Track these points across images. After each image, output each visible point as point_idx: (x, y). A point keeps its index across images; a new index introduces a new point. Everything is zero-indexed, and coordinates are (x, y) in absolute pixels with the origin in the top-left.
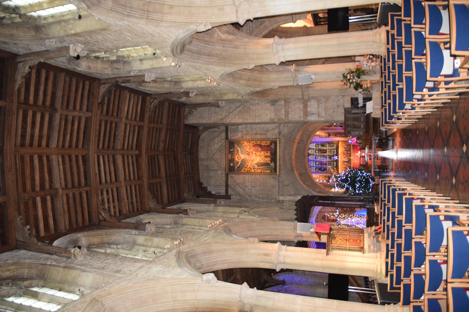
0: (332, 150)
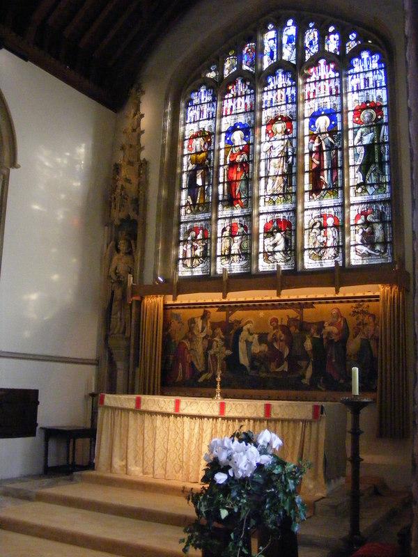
0: (330, 232)
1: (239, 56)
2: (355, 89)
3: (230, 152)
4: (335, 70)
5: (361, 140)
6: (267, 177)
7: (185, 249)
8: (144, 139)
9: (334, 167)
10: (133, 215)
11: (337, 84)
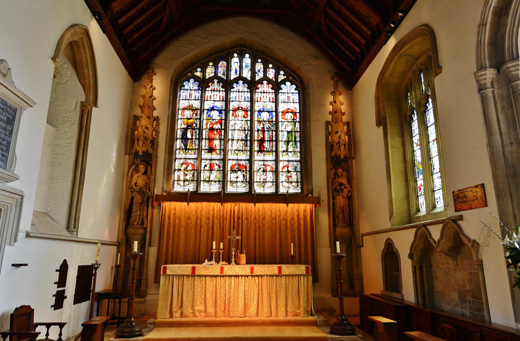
1: (216, 66)
2: (283, 101)
3: (210, 122)
4: (272, 89)
5: (285, 128)
6: (233, 140)
7: (179, 175)
8: (155, 103)
9: (271, 141)
10: (150, 150)
11: (273, 96)
